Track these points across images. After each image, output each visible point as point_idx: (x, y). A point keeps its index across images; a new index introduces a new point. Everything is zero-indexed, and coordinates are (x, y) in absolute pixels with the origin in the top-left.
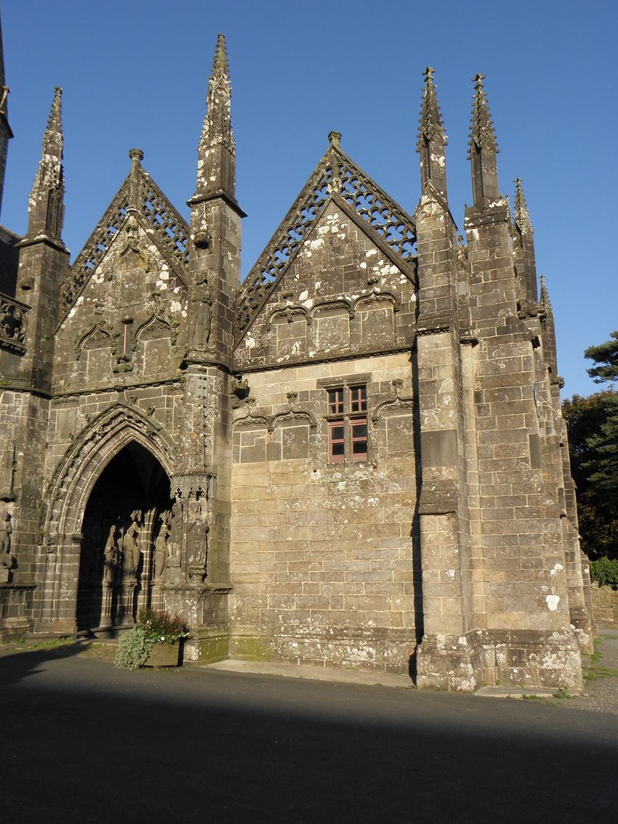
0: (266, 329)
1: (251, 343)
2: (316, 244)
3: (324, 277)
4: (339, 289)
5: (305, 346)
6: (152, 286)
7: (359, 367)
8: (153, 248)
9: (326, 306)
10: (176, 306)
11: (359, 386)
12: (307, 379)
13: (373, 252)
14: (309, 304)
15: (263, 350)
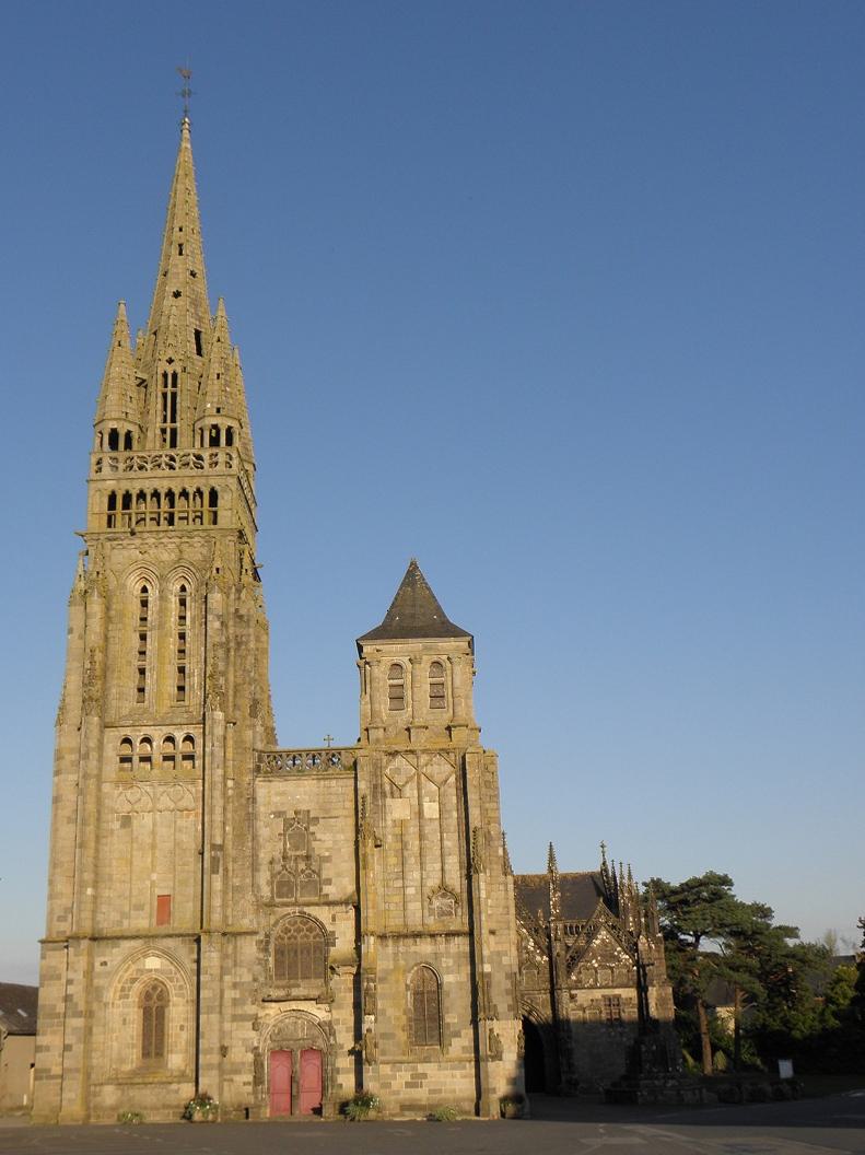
0: (580, 973)
1: (574, 978)
2: (598, 942)
3: (600, 955)
4: (607, 961)
5: (596, 981)
6: (526, 948)
7: (617, 991)
8: (524, 930)
9: (602, 967)
10: (538, 958)
11: (618, 997)
12: (598, 994)
13: (619, 949)
14: (596, 965)
15: (579, 981)
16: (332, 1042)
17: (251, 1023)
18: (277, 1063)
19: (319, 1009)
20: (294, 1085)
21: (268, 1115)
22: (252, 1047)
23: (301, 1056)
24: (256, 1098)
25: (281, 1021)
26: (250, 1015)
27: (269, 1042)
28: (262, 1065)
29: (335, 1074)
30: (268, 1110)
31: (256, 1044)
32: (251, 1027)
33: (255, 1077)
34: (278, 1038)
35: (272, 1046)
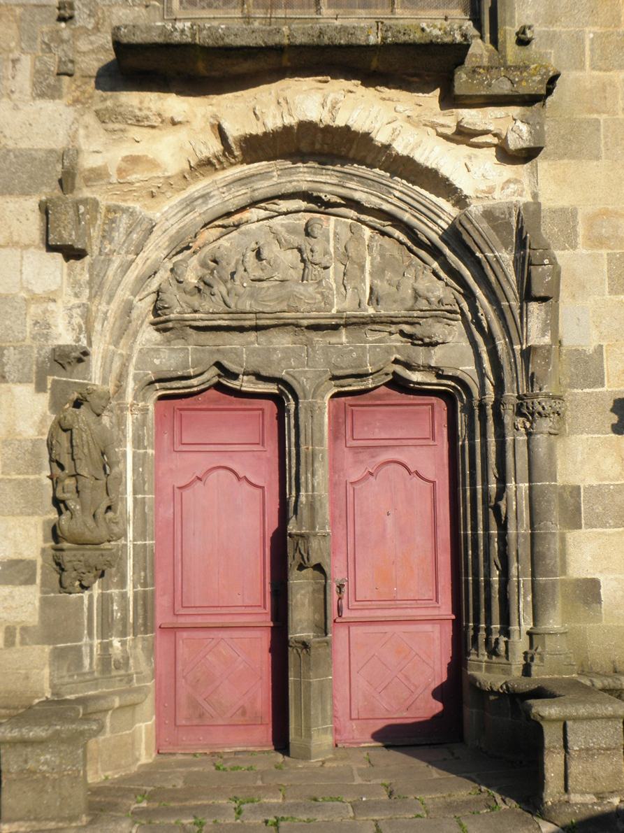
16: (536, 335)
17: (32, 203)
18: (201, 462)
19: (463, 135)
20: (301, 586)
21: (145, 756)
22: (39, 352)
23: (336, 435)
24: (66, 657)
25: (226, 219)
26: (26, 157)
27: (149, 335)
28: (106, 461)
29: (553, 525)
30: (144, 727)
31: (64, 336)
32: (32, 227)
33: (55, 534)
34: (209, 309)
35: (169, 358)
